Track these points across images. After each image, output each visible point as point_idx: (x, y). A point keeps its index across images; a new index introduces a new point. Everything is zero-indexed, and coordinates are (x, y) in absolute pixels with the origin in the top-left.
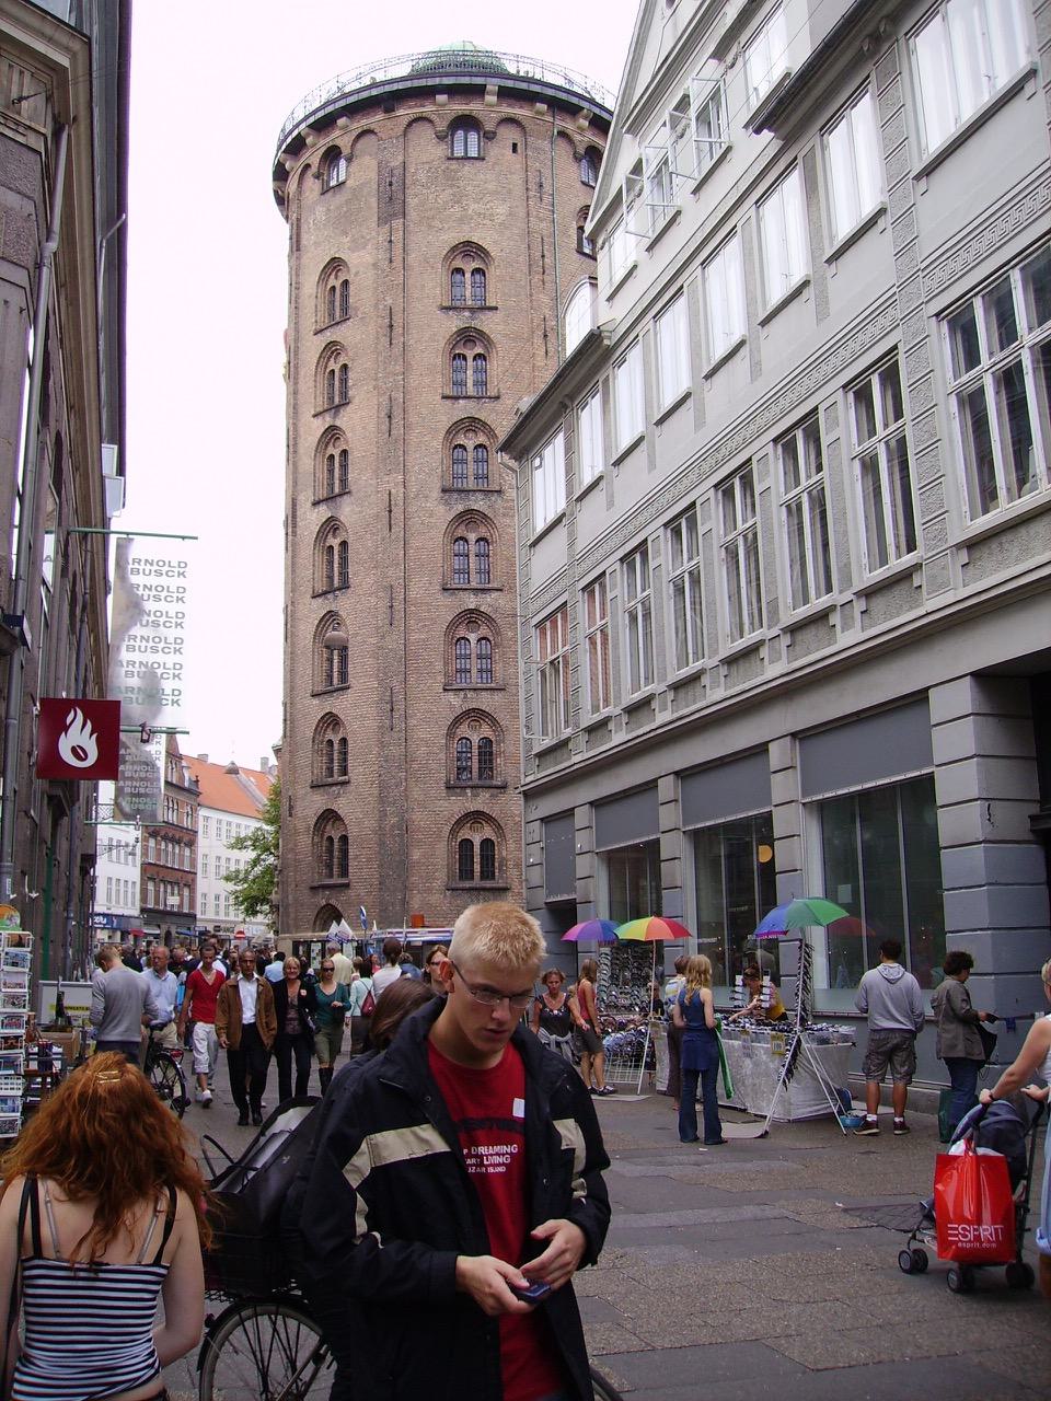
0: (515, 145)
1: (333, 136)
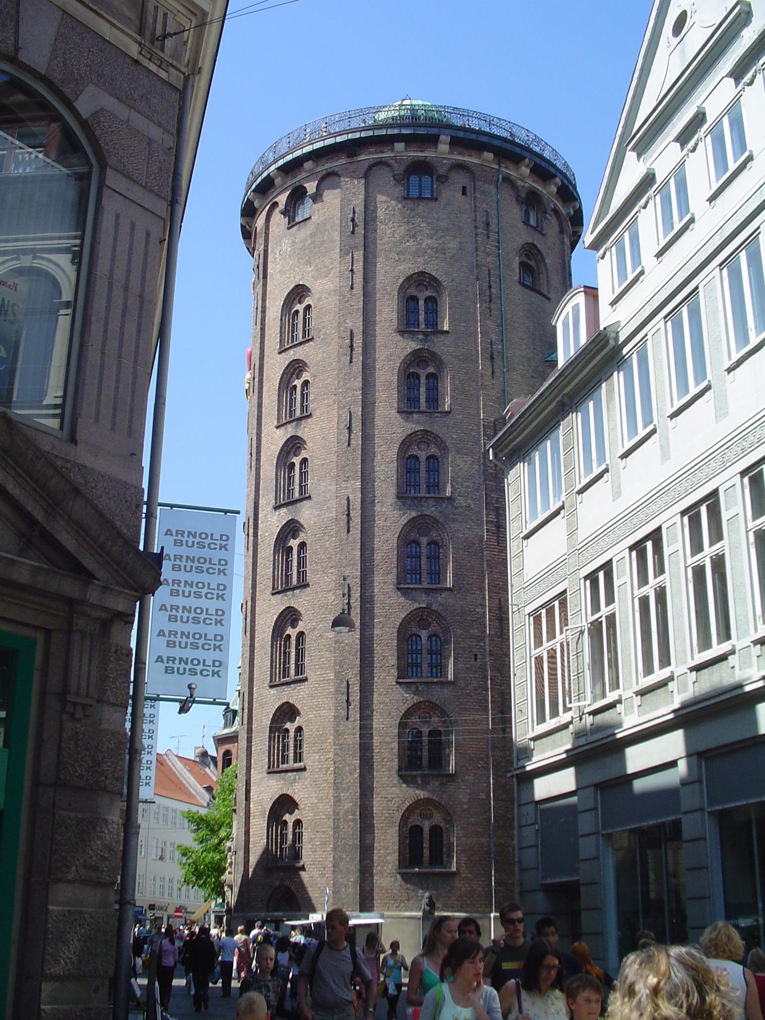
0: (464, 191)
1: (299, 178)
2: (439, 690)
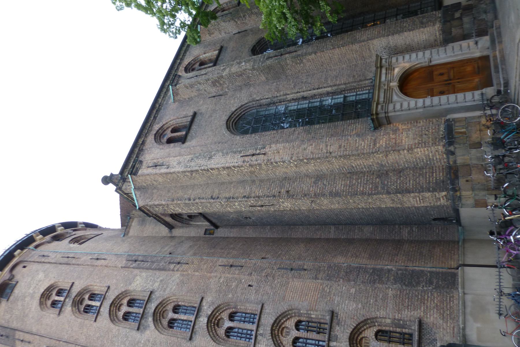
0: (24, 267)
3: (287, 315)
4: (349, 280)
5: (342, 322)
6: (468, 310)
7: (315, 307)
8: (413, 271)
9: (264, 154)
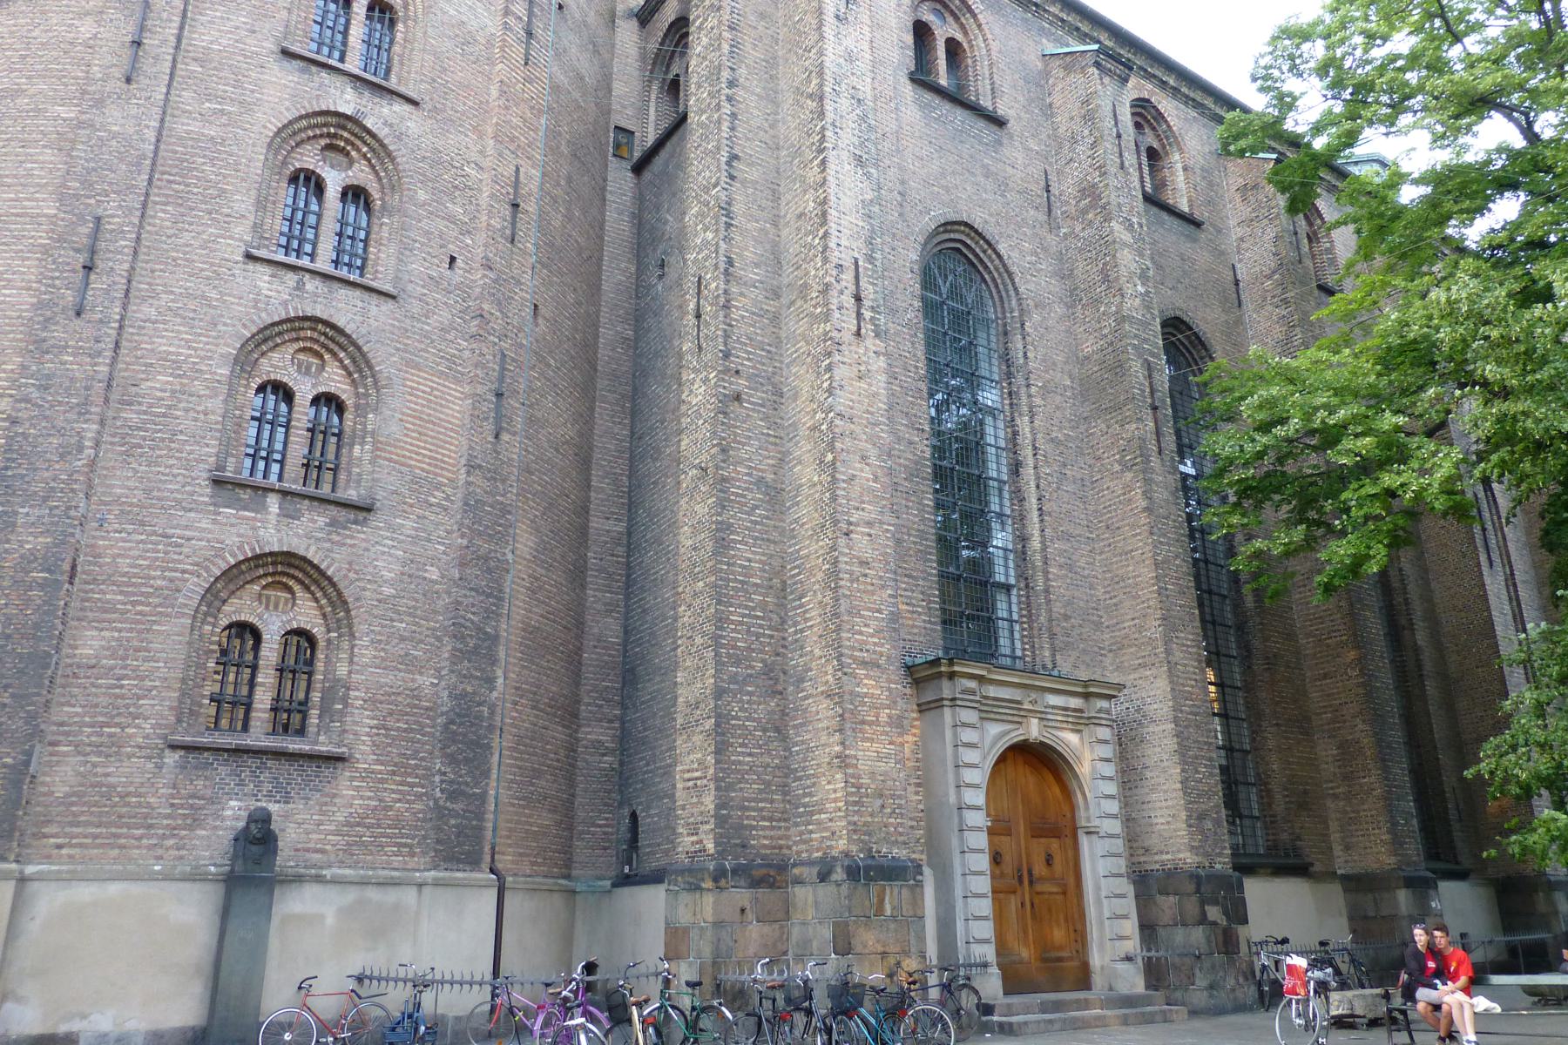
2: (360, 304)
3: (360, 371)
4: (463, 565)
5: (339, 534)
6: (373, 894)
7: (385, 459)
8: (489, 747)
9: (858, 333)
